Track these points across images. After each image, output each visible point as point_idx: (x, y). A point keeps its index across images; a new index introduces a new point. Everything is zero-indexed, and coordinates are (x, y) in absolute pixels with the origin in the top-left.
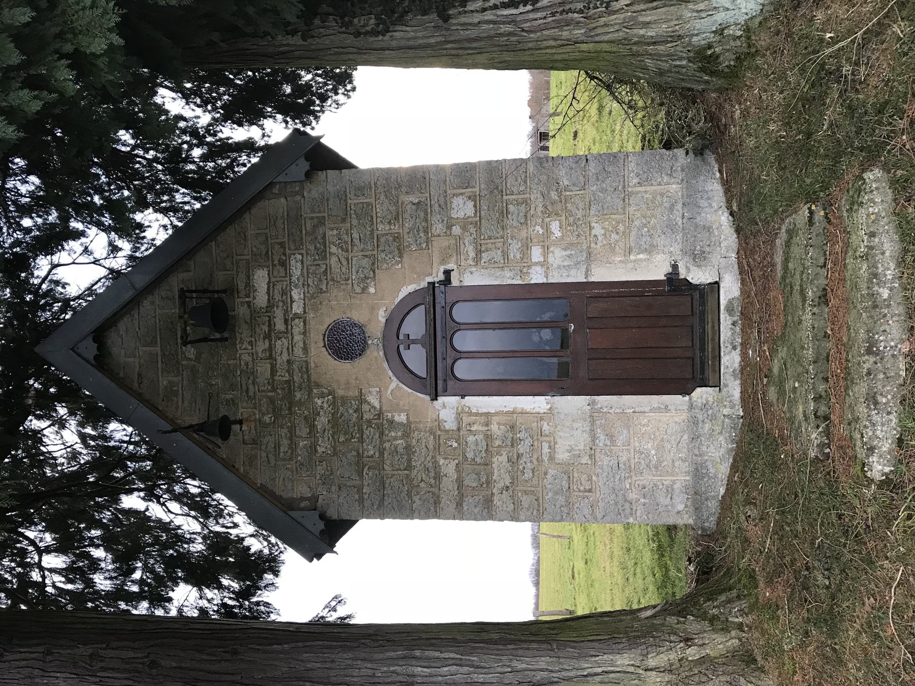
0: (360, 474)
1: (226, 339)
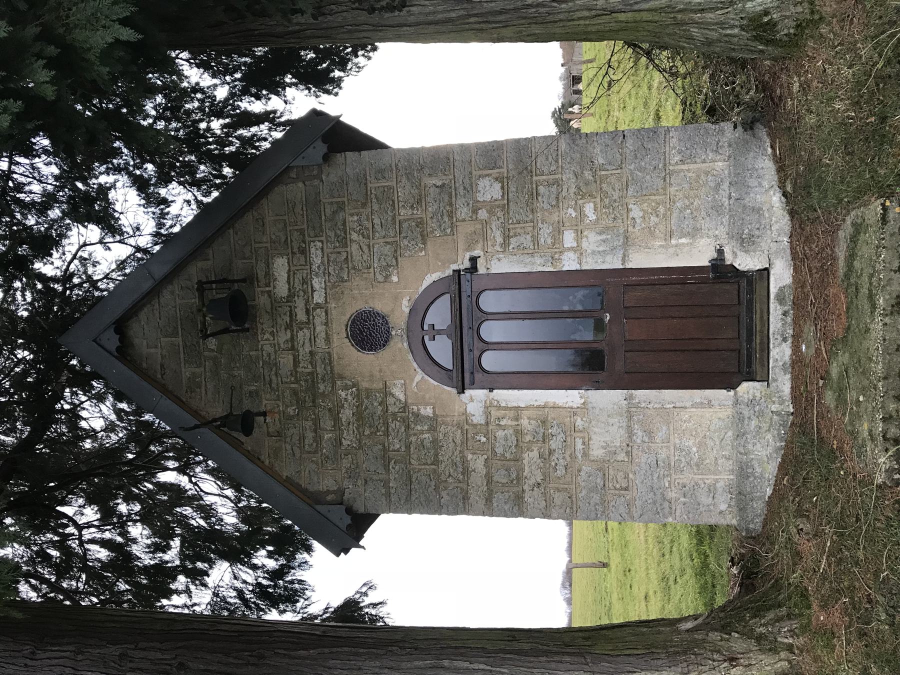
0: (387, 468)
1: (248, 330)
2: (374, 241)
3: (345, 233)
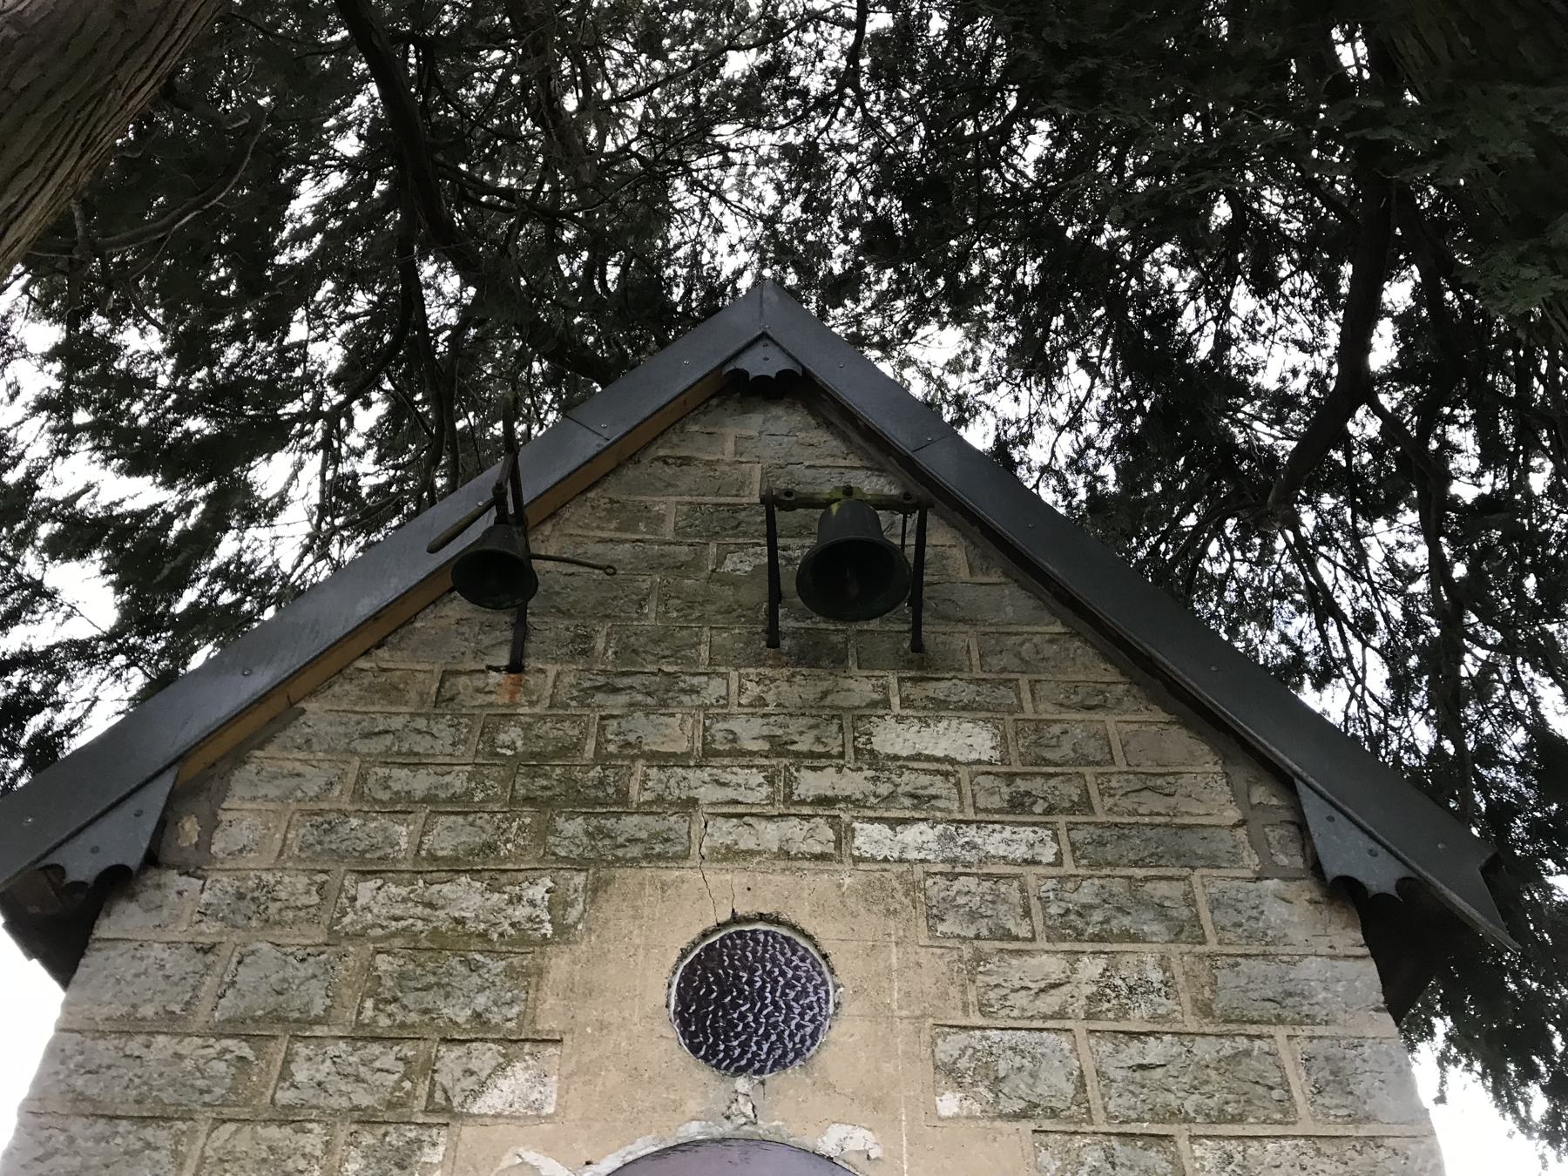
0: (235, 1028)
1: (773, 643)
2: (1081, 1033)
3: (1097, 938)
